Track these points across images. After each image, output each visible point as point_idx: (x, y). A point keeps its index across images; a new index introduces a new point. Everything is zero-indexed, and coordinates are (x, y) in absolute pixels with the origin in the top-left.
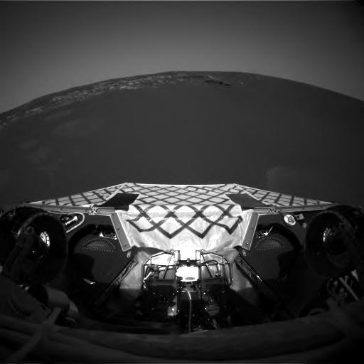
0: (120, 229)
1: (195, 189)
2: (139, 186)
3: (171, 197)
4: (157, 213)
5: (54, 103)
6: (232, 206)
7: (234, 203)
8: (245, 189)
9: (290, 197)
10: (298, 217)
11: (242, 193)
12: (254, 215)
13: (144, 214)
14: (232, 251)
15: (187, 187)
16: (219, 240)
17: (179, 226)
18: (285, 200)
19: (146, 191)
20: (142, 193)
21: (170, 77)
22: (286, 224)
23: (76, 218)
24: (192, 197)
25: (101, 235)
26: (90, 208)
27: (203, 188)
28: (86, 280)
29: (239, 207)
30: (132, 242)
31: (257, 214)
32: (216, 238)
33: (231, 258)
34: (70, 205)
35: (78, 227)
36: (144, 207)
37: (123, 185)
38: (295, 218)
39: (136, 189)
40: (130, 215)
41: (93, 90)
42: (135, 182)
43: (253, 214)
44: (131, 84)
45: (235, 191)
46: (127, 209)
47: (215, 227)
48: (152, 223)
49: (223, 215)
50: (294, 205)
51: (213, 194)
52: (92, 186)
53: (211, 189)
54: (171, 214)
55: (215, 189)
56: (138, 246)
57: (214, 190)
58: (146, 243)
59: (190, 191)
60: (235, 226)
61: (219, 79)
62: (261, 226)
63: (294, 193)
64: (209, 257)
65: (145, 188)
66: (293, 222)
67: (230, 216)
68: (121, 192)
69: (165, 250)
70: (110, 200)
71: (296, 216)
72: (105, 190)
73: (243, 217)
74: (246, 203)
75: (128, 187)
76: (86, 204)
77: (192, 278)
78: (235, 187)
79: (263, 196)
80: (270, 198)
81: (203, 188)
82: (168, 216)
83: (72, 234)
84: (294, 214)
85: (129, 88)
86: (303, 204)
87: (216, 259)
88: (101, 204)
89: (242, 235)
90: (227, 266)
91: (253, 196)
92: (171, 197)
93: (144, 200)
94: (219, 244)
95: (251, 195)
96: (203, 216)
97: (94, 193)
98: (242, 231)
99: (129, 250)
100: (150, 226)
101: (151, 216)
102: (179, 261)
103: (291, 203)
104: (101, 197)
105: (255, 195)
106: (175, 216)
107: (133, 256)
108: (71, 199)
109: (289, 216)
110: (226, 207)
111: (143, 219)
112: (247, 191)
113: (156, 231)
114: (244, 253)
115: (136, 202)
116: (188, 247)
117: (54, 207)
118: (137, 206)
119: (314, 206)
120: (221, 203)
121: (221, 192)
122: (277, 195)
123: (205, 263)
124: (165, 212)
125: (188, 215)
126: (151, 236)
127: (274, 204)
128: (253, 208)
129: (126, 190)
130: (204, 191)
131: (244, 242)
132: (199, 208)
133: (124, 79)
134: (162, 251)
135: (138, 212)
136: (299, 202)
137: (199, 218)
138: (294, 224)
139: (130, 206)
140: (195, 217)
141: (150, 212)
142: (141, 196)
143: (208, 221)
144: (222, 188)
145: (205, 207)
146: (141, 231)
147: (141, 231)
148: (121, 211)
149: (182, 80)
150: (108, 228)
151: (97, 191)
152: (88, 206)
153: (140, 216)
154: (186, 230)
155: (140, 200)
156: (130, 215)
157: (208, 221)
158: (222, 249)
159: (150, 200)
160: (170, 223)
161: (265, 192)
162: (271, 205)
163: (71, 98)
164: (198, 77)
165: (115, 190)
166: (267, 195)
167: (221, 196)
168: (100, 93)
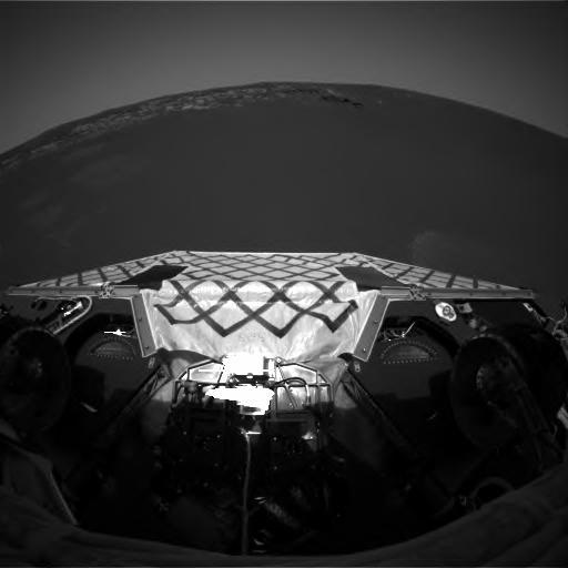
0: (143, 320)
1: (284, 259)
2: (193, 255)
3: (239, 269)
4: (207, 293)
6: (339, 284)
7: (344, 279)
9: (449, 276)
10: (462, 308)
11: (365, 266)
12: (381, 300)
13: (184, 295)
14: (336, 362)
16: (312, 342)
17: (244, 315)
18: (439, 280)
19: (203, 261)
20: (193, 265)
21: (265, 91)
22: (437, 315)
23: (79, 305)
24: (276, 269)
25: (118, 333)
26: (102, 288)
27: (299, 258)
28: (87, 407)
29: (354, 285)
30: (159, 342)
31: (385, 298)
32: (307, 336)
33: (334, 374)
34: (76, 285)
35: (78, 321)
36: (185, 285)
37: (168, 254)
38: (455, 308)
39: (186, 259)
40: (163, 297)
42: (188, 248)
43: (379, 297)
44: (201, 101)
45: (354, 263)
46: (158, 288)
47: (306, 318)
48: (198, 309)
49: (323, 298)
50: (454, 287)
51: (315, 266)
52: (117, 258)
54: (231, 296)
56: (170, 349)
57: (316, 260)
58: (178, 343)
60: (343, 317)
61: (338, 95)
62: (392, 321)
63: (456, 271)
64: (292, 372)
65: (200, 258)
66: (451, 315)
67: (336, 301)
68: (161, 264)
69: (211, 355)
70: (137, 276)
71: (458, 306)
72: (138, 263)
73: (358, 302)
74: (365, 280)
75: (172, 258)
76: (101, 283)
77: (253, 410)
79: (400, 272)
80: (415, 276)
81: (299, 258)
82: (225, 299)
83: (71, 330)
84: (455, 302)
86: (471, 287)
87: (303, 376)
89: (353, 336)
90: (325, 388)
91: (384, 272)
92: (239, 269)
93: (194, 274)
94: (311, 349)
95: (379, 270)
96: (285, 299)
97: (119, 267)
98: (355, 326)
99: (152, 356)
100: (194, 315)
101: (196, 298)
102: (236, 376)
103: (450, 284)
104: (126, 272)
106: (236, 299)
107: (158, 367)
108: (80, 279)
109: (444, 304)
110: (328, 285)
111: (183, 303)
112: (375, 263)
114: (357, 367)
115: (179, 277)
116: (246, 355)
117: (51, 289)
118: (176, 285)
119: (491, 291)
120: (324, 279)
121: (328, 264)
122: (427, 271)
123: (284, 381)
124: (221, 292)
125: (258, 297)
126: (189, 330)
127: (418, 284)
128: (378, 289)
129: (169, 261)
130: (300, 262)
131: (358, 346)
132: (280, 285)
133: (191, 94)
134: (206, 358)
135: (176, 293)
136: (464, 283)
137: (280, 303)
138: (454, 318)
139: (165, 283)
140: (273, 300)
141: (194, 292)
142: (190, 268)
143: (295, 307)
144: (332, 259)
145: (291, 284)
146: (173, 321)
147: (173, 321)
148: (147, 290)
149: (283, 96)
150: (124, 317)
151: (122, 265)
152: (100, 284)
153: (178, 299)
154: (254, 325)
156: (163, 297)
157: (295, 307)
158: (318, 357)
159: (196, 275)
160: (227, 311)
161: (406, 266)
162: (413, 286)
163: (103, 125)
164: (311, 91)
165: (151, 262)
166: (409, 270)
168: (150, 116)
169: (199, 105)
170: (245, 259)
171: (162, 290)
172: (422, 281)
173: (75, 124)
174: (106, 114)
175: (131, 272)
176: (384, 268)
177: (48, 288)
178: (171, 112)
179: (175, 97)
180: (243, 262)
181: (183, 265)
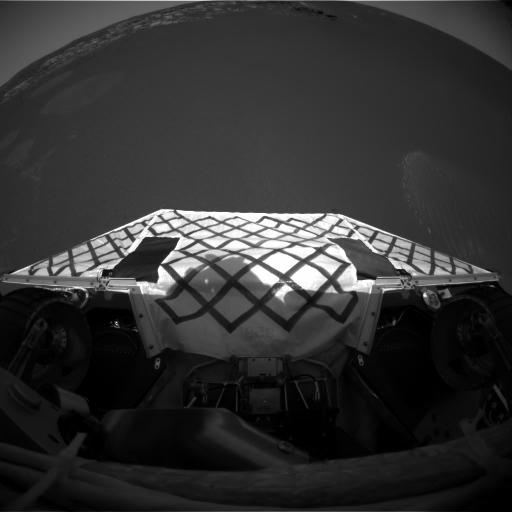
1: (273, 224)
2: (181, 217)
5: (46, 68)
8: (357, 227)
10: (443, 294)
15: (264, 217)
17: (249, 305)
19: (193, 227)
20: (187, 236)
31: (379, 288)
37: (154, 216)
39: (176, 224)
41: (108, 35)
42: (175, 207)
53: (301, 225)
55: (309, 225)
59: (266, 228)
61: (320, 9)
68: (151, 235)
71: (440, 292)
72: (126, 230)
75: (160, 221)
78: (341, 221)
85: (164, 23)
88: (111, 266)
91: (370, 246)
95: (367, 244)
100: (198, 306)
104: (117, 249)
105: (375, 243)
109: (431, 292)
112: (362, 232)
113: (207, 317)
115: (172, 255)
128: (374, 278)
129: (160, 229)
130: (290, 230)
133: (158, 12)
139: (161, 271)
144: (320, 224)
146: (178, 320)
147: (178, 320)
149: (254, 7)
155: (182, 251)
161: (386, 237)
167: (319, 240)
168: (116, 38)
169: (168, 18)
170: (236, 223)
171: (160, 281)
172: (409, 262)
173: (44, 59)
174: (73, 44)
175: (122, 250)
176: (371, 240)
177: (40, 273)
178: (139, 29)
179: (143, 17)
180: (234, 228)
181: (173, 236)
